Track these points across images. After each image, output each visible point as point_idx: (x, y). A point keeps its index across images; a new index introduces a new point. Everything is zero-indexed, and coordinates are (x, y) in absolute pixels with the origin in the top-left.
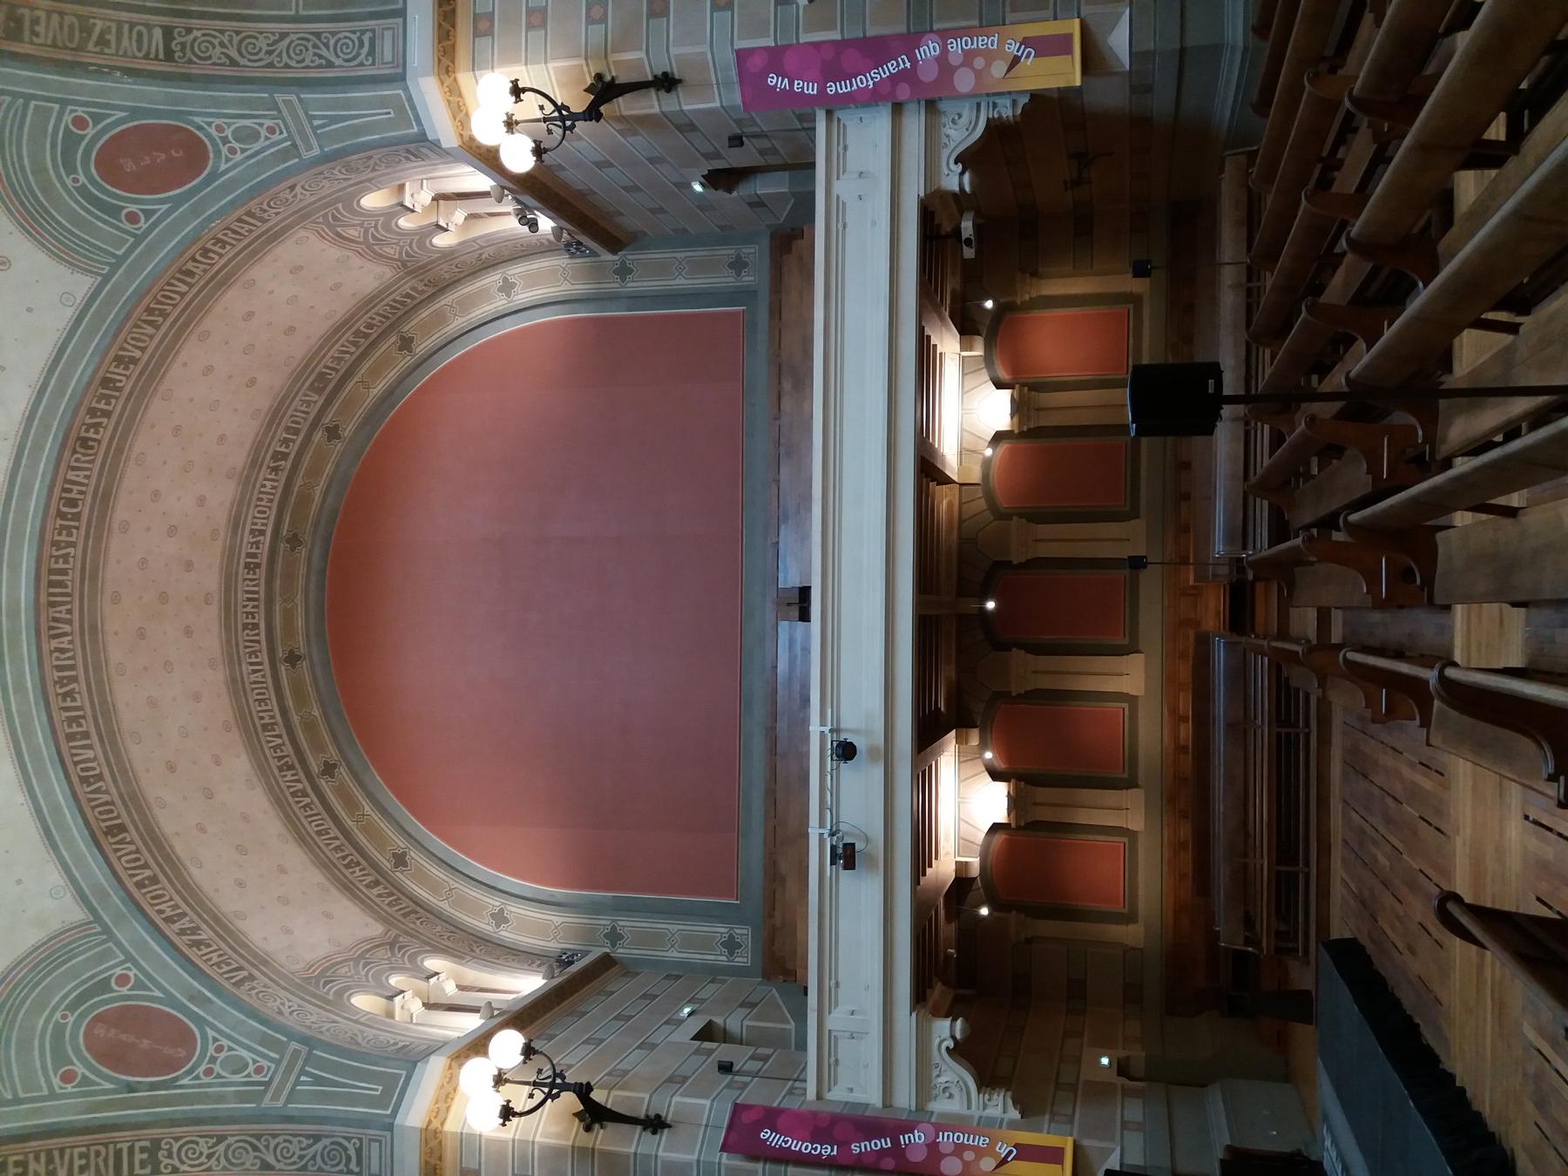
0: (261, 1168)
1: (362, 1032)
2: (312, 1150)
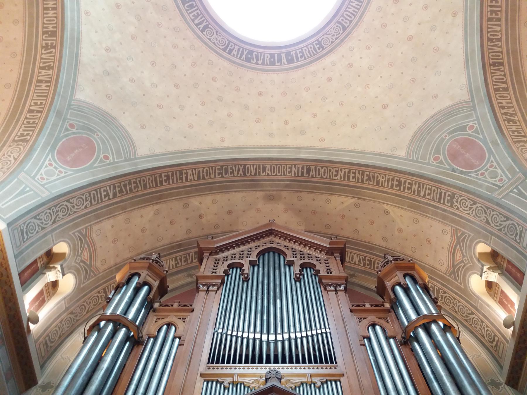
0: (485, 222)
2: (504, 224)
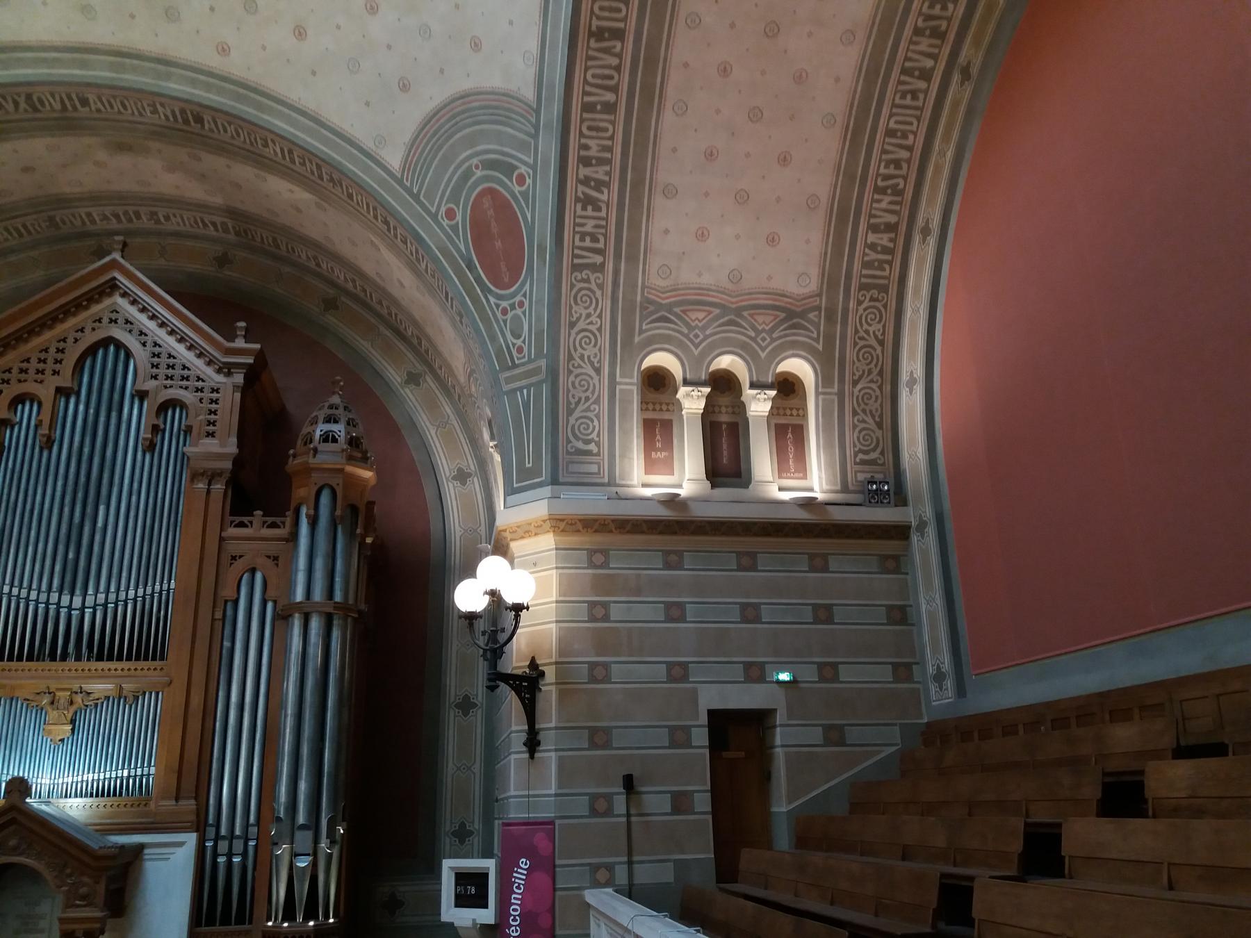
1: (597, 401)
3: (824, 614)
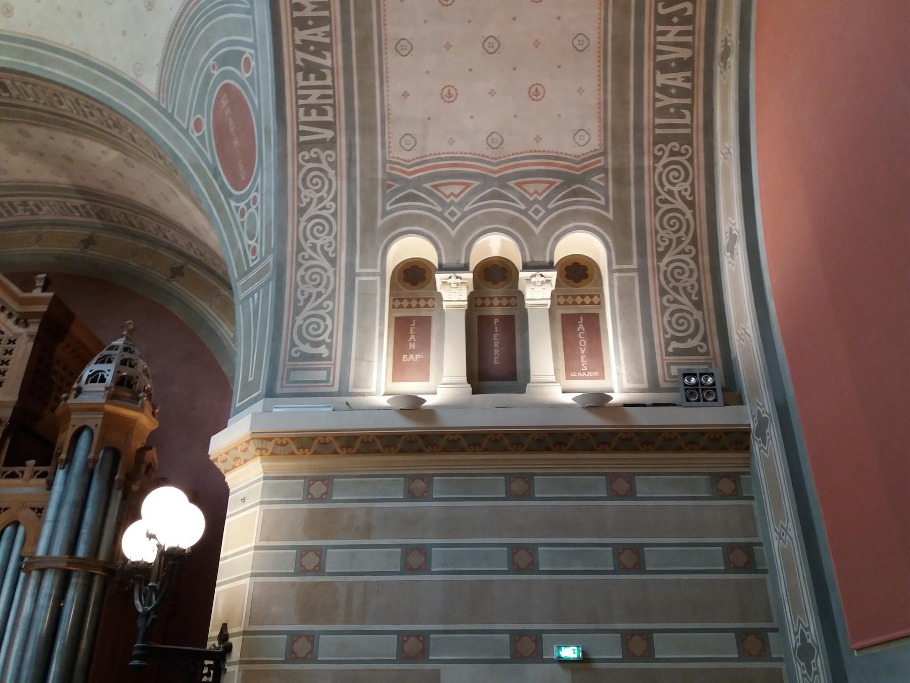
1: (332, 297)
3: (631, 559)
